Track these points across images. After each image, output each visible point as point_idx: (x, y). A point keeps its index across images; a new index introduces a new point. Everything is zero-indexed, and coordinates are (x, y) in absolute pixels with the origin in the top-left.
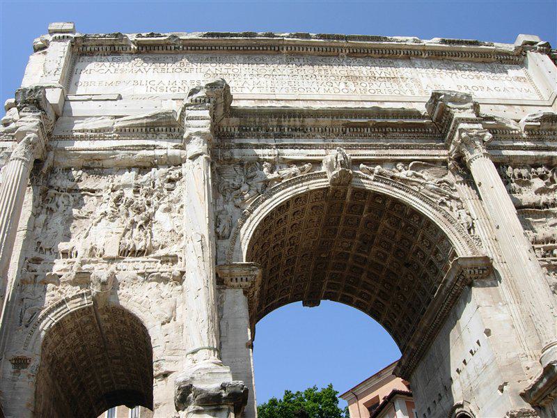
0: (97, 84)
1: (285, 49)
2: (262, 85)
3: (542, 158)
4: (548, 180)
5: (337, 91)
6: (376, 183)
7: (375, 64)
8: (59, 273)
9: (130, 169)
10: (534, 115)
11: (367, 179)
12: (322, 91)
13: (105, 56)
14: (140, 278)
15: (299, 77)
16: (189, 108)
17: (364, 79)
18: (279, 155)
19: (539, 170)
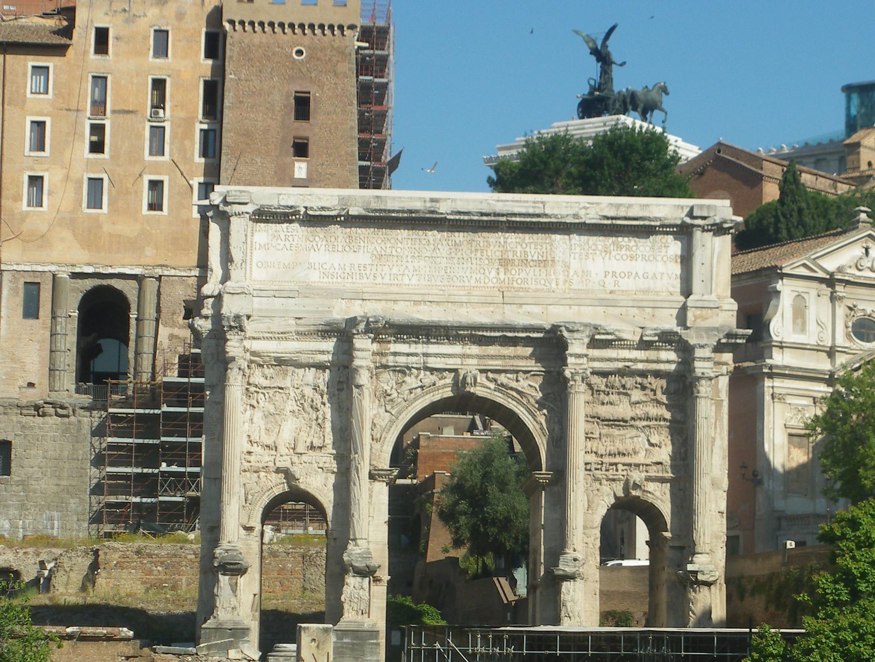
0: (276, 266)
1: (447, 224)
2: (422, 272)
3: (649, 371)
4: (648, 392)
5: (487, 281)
6: (496, 393)
7: (531, 240)
8: (267, 465)
9: (310, 366)
10: (655, 329)
11: (490, 389)
12: (473, 281)
13: (279, 223)
14: (320, 470)
15: (455, 260)
16: (356, 336)
17: (517, 261)
18: (424, 363)
19: (645, 381)
